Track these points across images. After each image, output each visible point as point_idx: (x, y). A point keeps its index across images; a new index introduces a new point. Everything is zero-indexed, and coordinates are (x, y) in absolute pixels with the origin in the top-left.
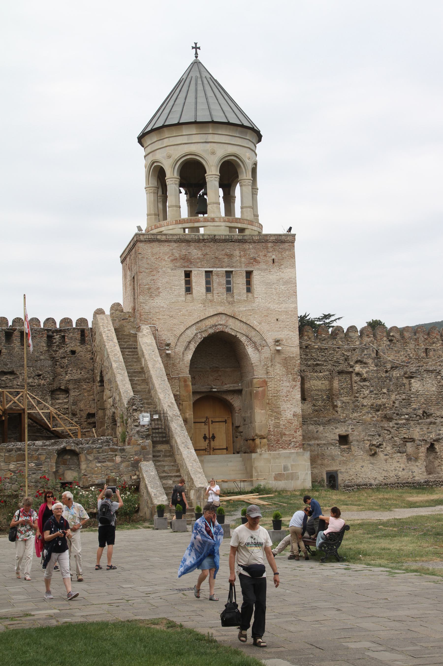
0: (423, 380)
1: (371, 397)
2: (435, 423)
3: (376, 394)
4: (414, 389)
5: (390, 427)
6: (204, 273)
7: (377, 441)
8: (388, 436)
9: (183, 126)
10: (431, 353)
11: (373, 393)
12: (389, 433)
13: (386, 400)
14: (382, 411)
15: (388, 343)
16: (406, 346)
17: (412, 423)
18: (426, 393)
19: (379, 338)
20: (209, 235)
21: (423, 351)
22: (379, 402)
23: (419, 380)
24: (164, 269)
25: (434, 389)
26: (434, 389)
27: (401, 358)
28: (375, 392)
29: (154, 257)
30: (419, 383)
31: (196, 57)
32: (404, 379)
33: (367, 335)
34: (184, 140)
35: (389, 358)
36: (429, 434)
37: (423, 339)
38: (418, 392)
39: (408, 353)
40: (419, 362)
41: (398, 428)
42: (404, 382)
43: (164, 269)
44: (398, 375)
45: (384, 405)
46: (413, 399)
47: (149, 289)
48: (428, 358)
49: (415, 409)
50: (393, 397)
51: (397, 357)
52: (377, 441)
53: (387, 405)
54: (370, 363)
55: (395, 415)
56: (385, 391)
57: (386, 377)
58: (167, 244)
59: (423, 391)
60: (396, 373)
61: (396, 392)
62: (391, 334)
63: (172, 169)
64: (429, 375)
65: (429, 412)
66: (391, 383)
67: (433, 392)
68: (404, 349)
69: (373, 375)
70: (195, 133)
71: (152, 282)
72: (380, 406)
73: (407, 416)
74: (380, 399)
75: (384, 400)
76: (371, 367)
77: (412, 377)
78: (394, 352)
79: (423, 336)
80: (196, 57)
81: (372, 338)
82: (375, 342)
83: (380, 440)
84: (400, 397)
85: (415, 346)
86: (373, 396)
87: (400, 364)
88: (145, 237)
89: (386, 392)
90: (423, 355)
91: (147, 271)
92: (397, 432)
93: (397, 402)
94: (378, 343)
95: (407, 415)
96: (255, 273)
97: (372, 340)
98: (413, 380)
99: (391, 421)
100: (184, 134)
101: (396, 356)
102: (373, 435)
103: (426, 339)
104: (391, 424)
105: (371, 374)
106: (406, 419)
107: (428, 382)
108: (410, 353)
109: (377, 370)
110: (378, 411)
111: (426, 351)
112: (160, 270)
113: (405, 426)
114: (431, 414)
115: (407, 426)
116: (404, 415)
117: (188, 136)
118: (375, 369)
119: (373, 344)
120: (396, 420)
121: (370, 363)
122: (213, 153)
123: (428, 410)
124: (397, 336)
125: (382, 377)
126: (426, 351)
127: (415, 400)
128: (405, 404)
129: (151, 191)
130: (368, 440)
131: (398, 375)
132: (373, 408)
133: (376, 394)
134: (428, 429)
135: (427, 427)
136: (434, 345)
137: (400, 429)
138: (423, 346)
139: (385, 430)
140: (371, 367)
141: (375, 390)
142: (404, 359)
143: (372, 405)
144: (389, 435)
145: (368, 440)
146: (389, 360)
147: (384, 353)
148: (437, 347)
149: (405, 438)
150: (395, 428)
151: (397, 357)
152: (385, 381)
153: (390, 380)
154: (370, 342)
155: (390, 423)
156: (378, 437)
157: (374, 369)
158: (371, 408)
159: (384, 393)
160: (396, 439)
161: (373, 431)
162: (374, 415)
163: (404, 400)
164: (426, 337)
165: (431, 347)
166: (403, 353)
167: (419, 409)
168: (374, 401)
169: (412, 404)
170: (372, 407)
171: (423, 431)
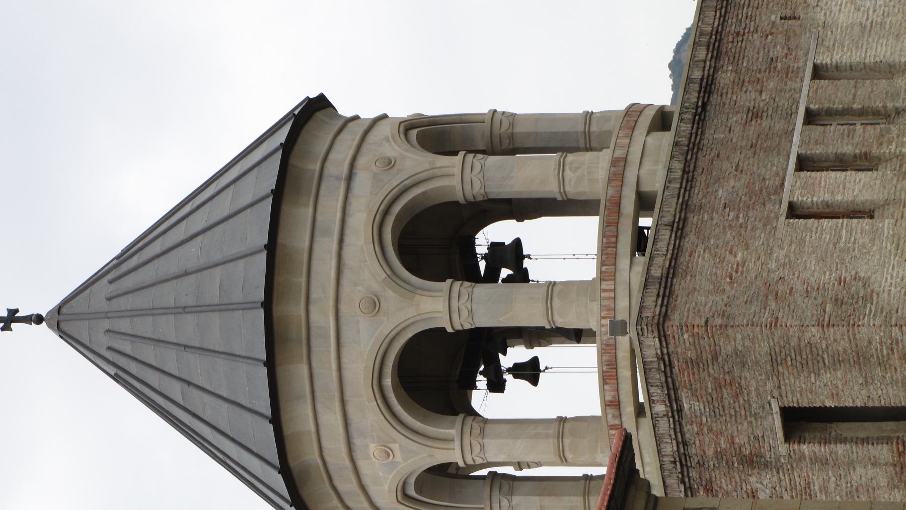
6: (803, 174)
9: (281, 239)
20: (672, 157)
24: (773, 265)
29: (728, 288)
31: (39, 319)
34: (326, 247)
43: (773, 265)
47: (838, 302)
58: (684, 258)
63: (419, 291)
70: (310, 210)
71: (814, 294)
80: (39, 319)
88: (650, 301)
91: (773, 305)
96: (824, 59)
100: (307, 244)
112: (775, 276)
117: (317, 233)
122: (390, 164)
129: (476, 431)
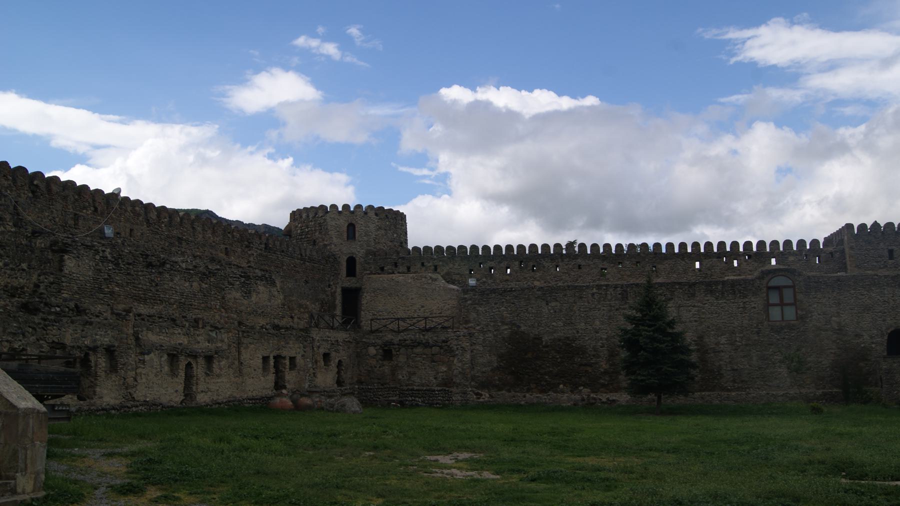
0: (78, 257)
1: (5, 273)
2: (91, 323)
3: (12, 269)
4: (67, 269)
5: (34, 322)
7: (20, 343)
8: (33, 337)
10: (81, 222)
11: (8, 267)
12: (34, 332)
13: (25, 281)
14: (18, 298)
15: (30, 195)
16: (52, 205)
17: (65, 320)
18: (81, 278)
19: (19, 184)
21: (71, 216)
22: (15, 283)
23: (74, 257)
25: (90, 273)
26: (90, 273)
27: (44, 220)
28: (11, 266)
30: (74, 261)
32: (50, 253)
33: (4, 176)
35: (30, 218)
36: (84, 339)
37: (72, 199)
38: (71, 275)
39: (53, 215)
40: (65, 232)
41: (46, 326)
42: (50, 257)
44: (43, 245)
45: (22, 288)
46: (64, 284)
48: (76, 228)
49: (65, 300)
50: (34, 278)
51: (40, 219)
52: (20, 343)
53: (26, 289)
54: (8, 220)
55: (42, 305)
56: (24, 266)
57: (26, 245)
59: (77, 274)
60: (40, 243)
61: (39, 271)
62: (35, 182)
64: (86, 252)
65: (82, 307)
66: (33, 256)
67: (88, 278)
68: (50, 208)
69: (9, 238)
72: (17, 289)
73: (58, 309)
74: (16, 278)
75: (21, 280)
76: (7, 226)
77: (66, 252)
78: (37, 210)
79: (73, 196)
81: (9, 182)
82: (14, 189)
83: (23, 342)
84: (46, 279)
85: (63, 207)
86: (8, 272)
87: (42, 229)
89: (26, 268)
90: (71, 222)
92: (45, 332)
93: (42, 286)
94: (18, 192)
95: (58, 307)
97: (10, 185)
98: (66, 257)
99: (35, 315)
101: (38, 217)
102: (15, 334)
103: (77, 200)
104: (37, 319)
105: (7, 236)
106: (56, 313)
107: (84, 262)
108: (56, 215)
109: (15, 232)
110: (13, 296)
111: (76, 218)
113: (55, 324)
114: (84, 310)
115: (58, 324)
116: (55, 307)
118: (13, 230)
119: (11, 191)
120: (44, 313)
121: (8, 220)
123: (81, 303)
124: (42, 186)
125: (22, 244)
126: (76, 218)
127: (67, 286)
128: (54, 290)
130: (7, 341)
131: (43, 245)
132: (6, 291)
133: (12, 269)
134: (83, 331)
135: (81, 328)
136: (84, 211)
137: (49, 328)
138: (71, 210)
139: (30, 327)
140: (7, 226)
141: (11, 263)
142: (48, 224)
143: (6, 286)
144: (33, 335)
145: (7, 341)
146: (30, 222)
147: (24, 210)
148: (88, 215)
149: (53, 342)
150: (41, 326)
151: (40, 219)
152: (26, 252)
153: (32, 252)
154: (7, 187)
155: (35, 317)
156: (21, 337)
157: (12, 230)
158: (4, 290)
159: (23, 270)
160: (41, 342)
161: (15, 327)
162: (7, 302)
163: (52, 283)
164: (76, 197)
165: (80, 214)
166: (47, 214)
167: (71, 300)
168: (9, 281)
169: (62, 291)
170: (6, 289)
171: (76, 334)
